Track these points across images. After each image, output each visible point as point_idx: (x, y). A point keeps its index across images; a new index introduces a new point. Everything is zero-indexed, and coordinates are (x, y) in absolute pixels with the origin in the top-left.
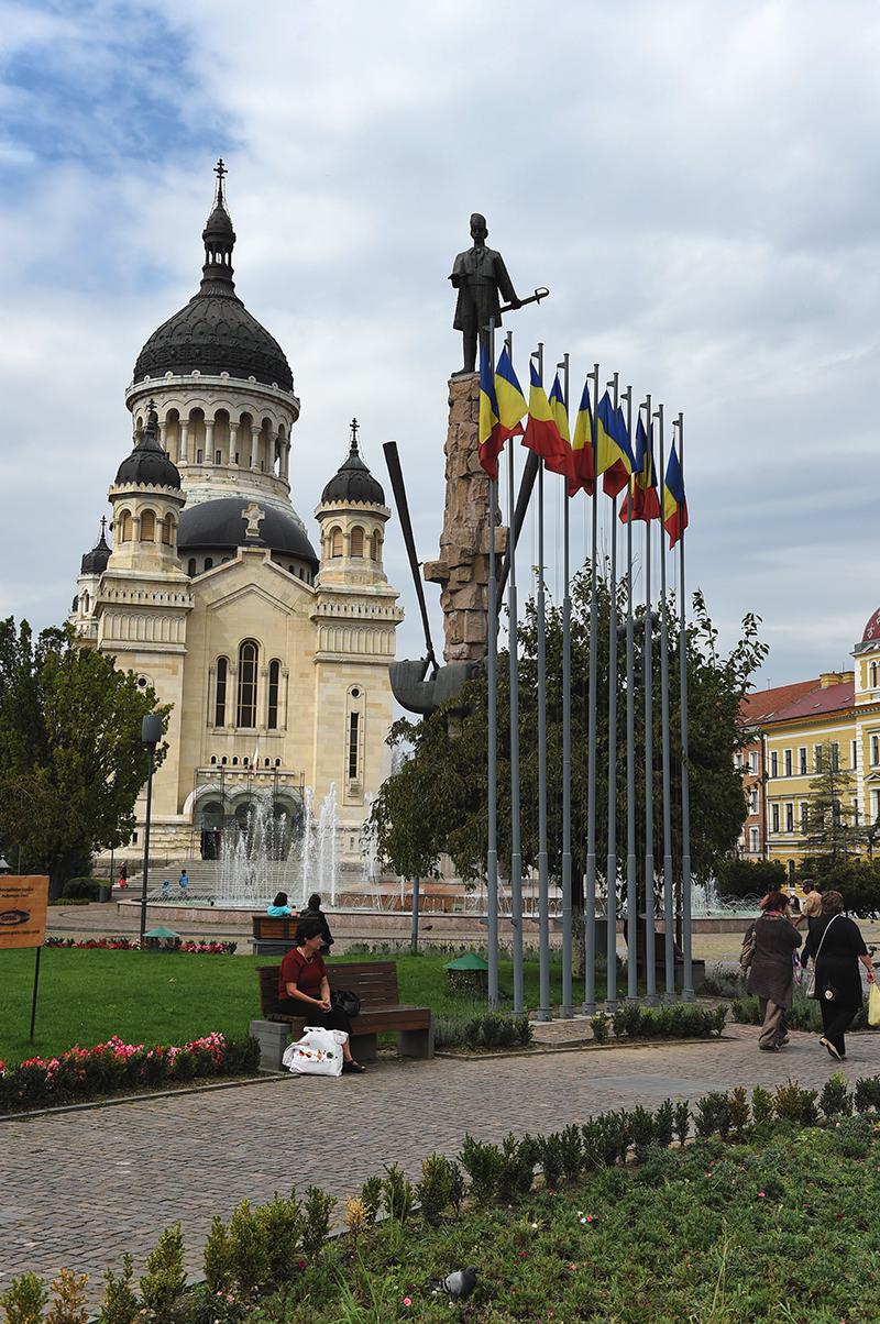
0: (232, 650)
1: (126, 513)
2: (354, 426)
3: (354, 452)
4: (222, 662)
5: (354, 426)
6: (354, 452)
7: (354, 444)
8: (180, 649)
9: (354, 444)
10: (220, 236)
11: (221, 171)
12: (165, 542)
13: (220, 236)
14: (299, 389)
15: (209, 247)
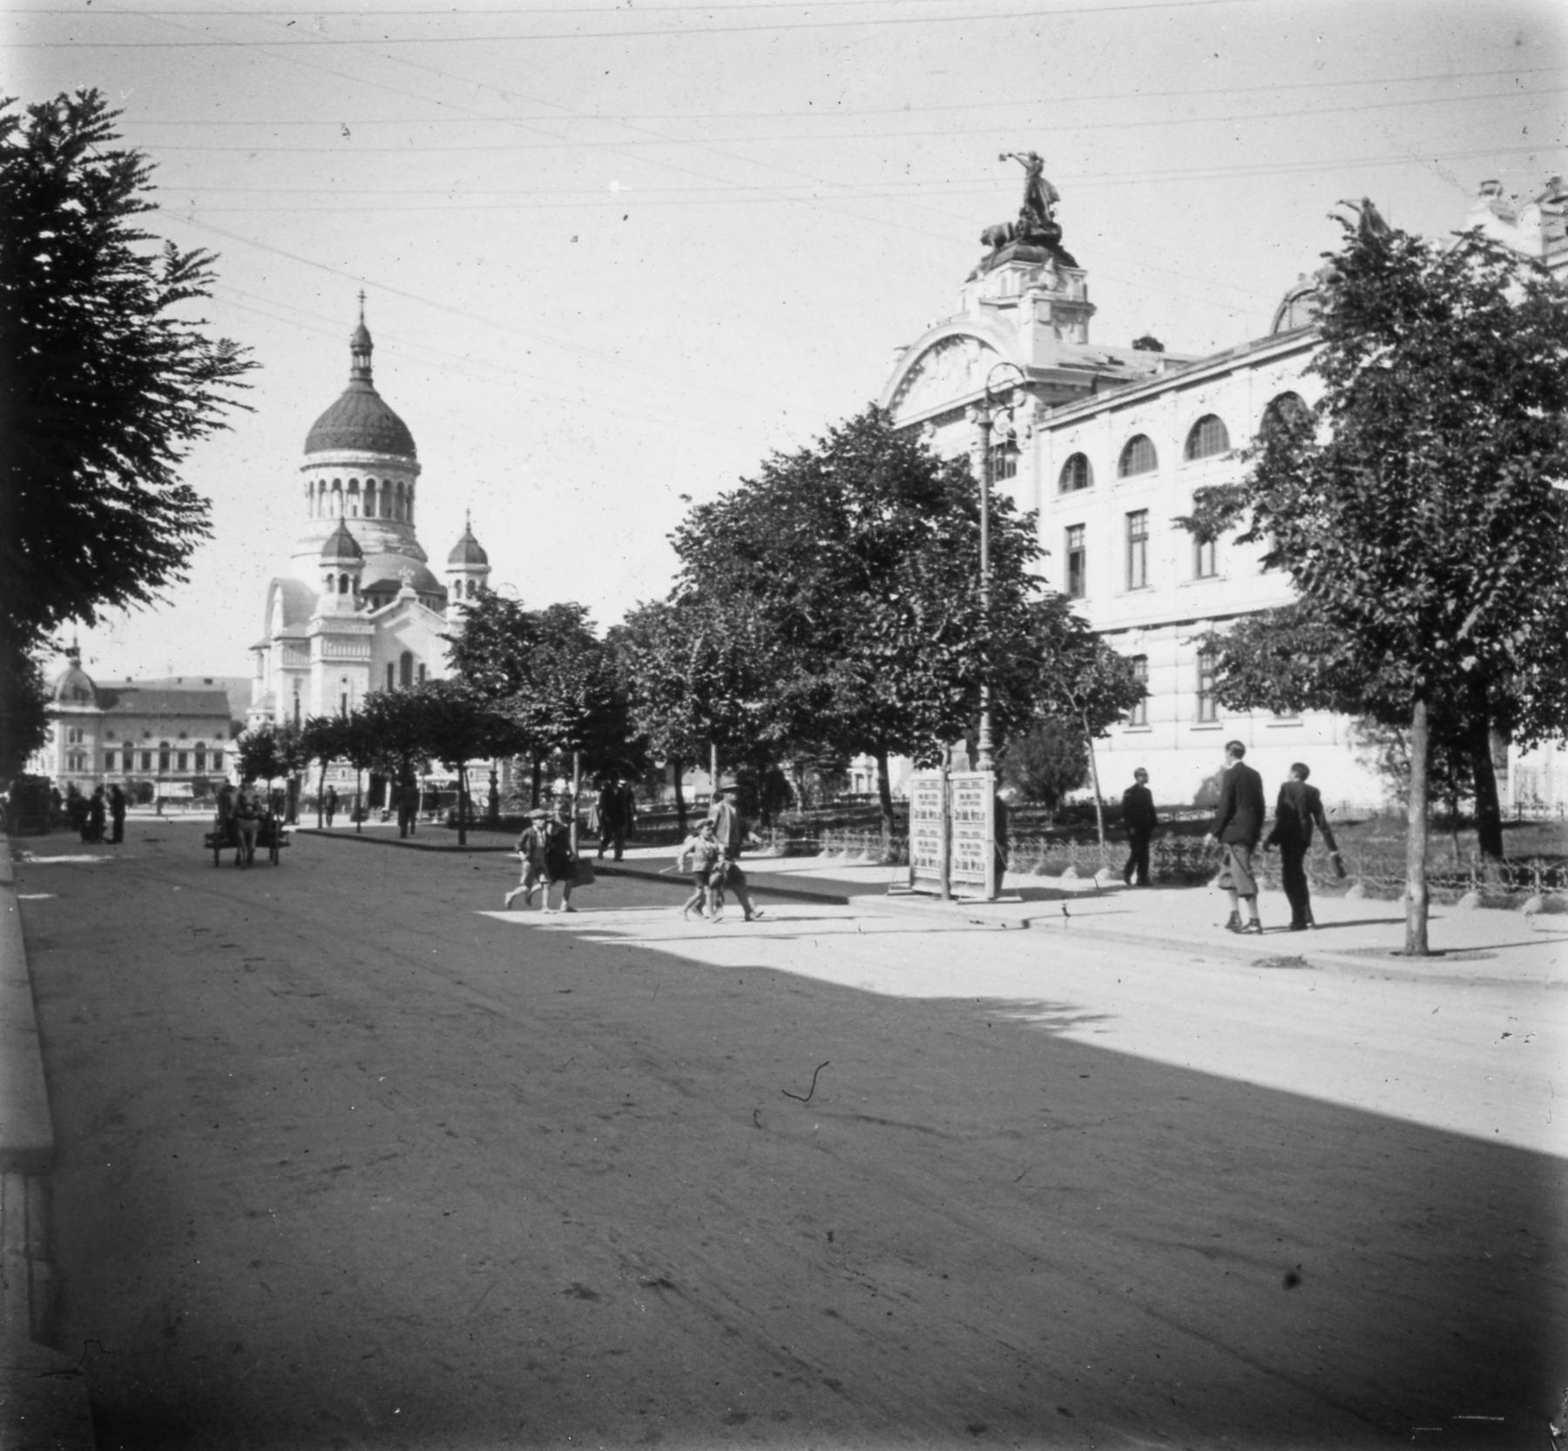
0: (396, 658)
1: (330, 576)
2: (468, 512)
3: (468, 530)
4: (390, 667)
5: (468, 512)
6: (468, 530)
7: (468, 524)
8: (367, 660)
9: (468, 524)
10: (363, 346)
11: (362, 297)
12: (355, 592)
13: (363, 346)
14: (421, 458)
15: (356, 354)
